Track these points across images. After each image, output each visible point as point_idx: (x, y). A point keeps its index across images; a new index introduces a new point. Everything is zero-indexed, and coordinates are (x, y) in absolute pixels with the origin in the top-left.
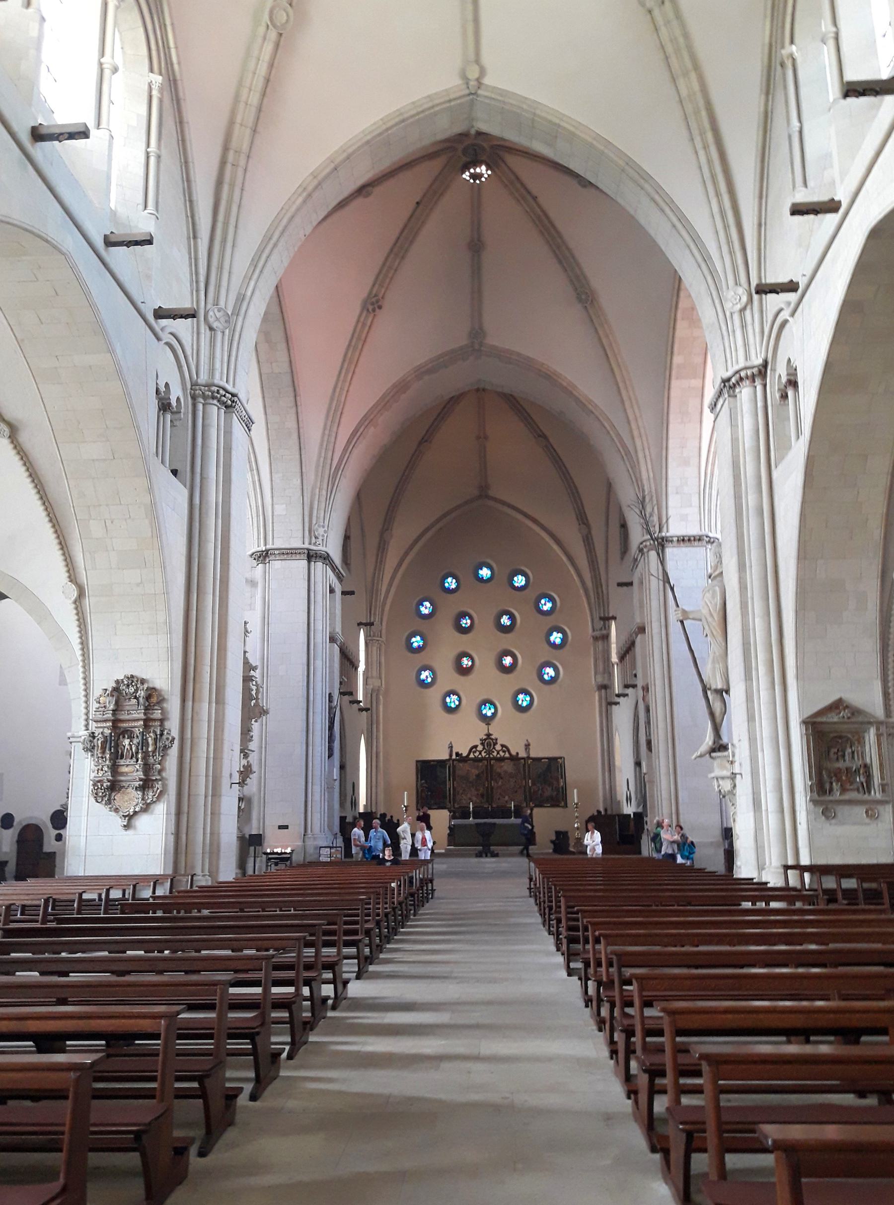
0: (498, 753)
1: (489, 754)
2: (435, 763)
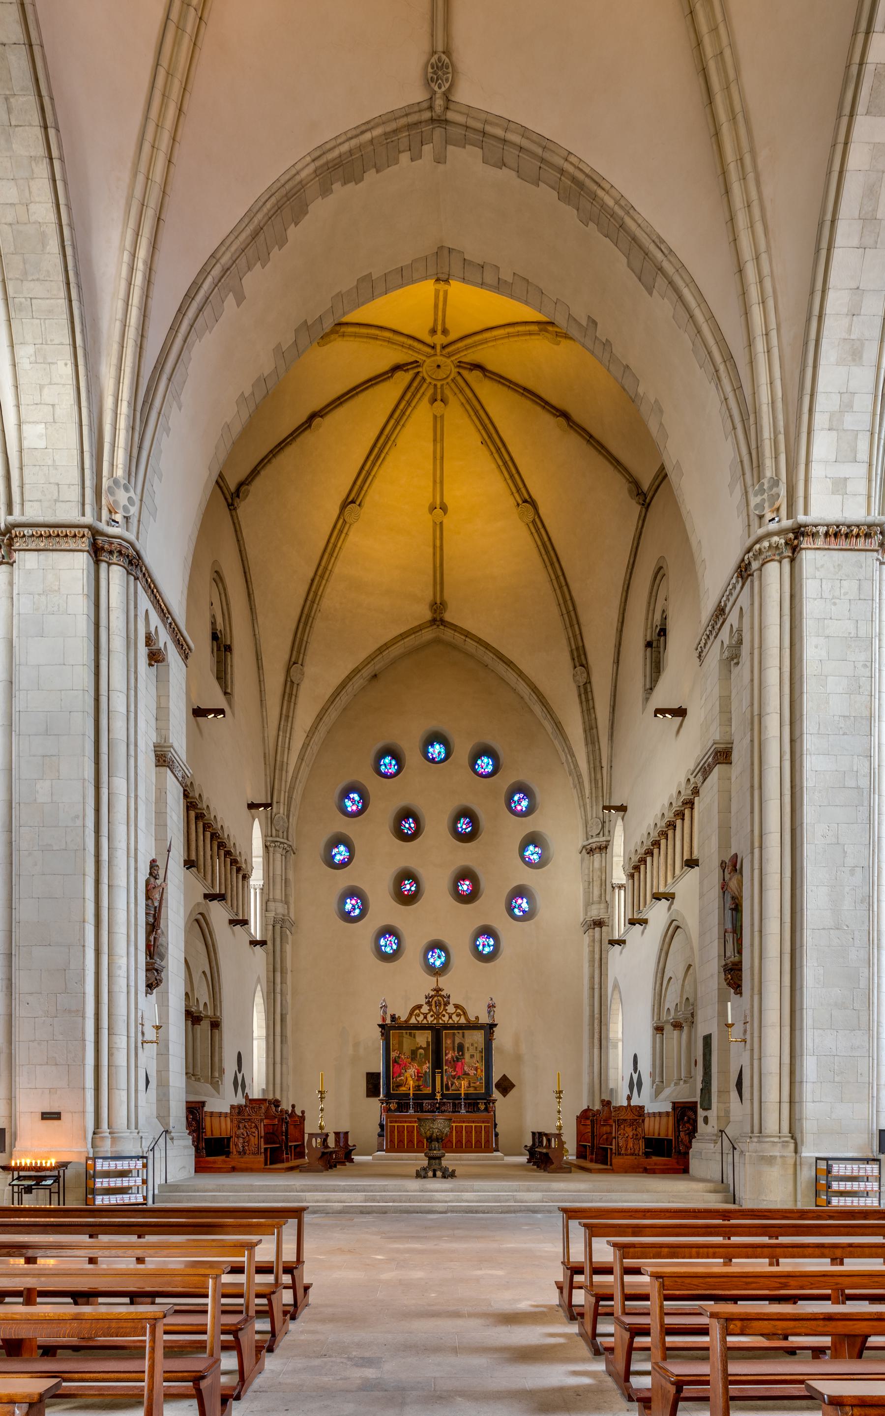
0: (450, 1017)
1: (438, 1018)
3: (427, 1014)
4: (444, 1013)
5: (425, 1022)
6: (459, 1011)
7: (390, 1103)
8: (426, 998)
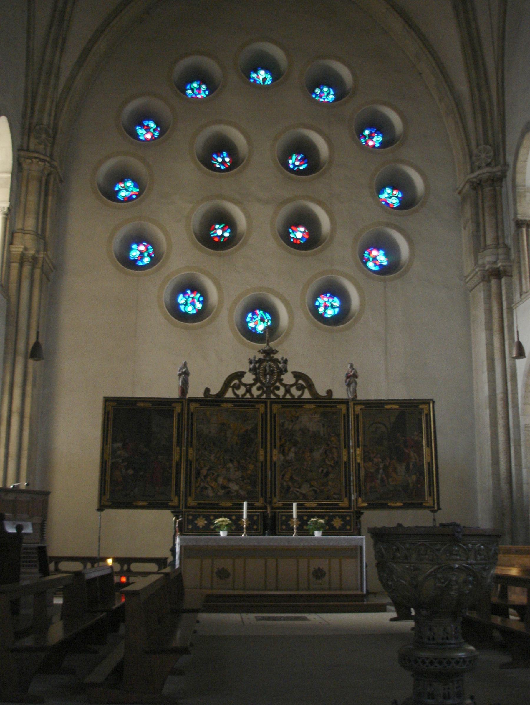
0: (288, 391)
2: (149, 405)
3: (252, 385)
5: (248, 396)
6: (300, 382)
8: (251, 362)
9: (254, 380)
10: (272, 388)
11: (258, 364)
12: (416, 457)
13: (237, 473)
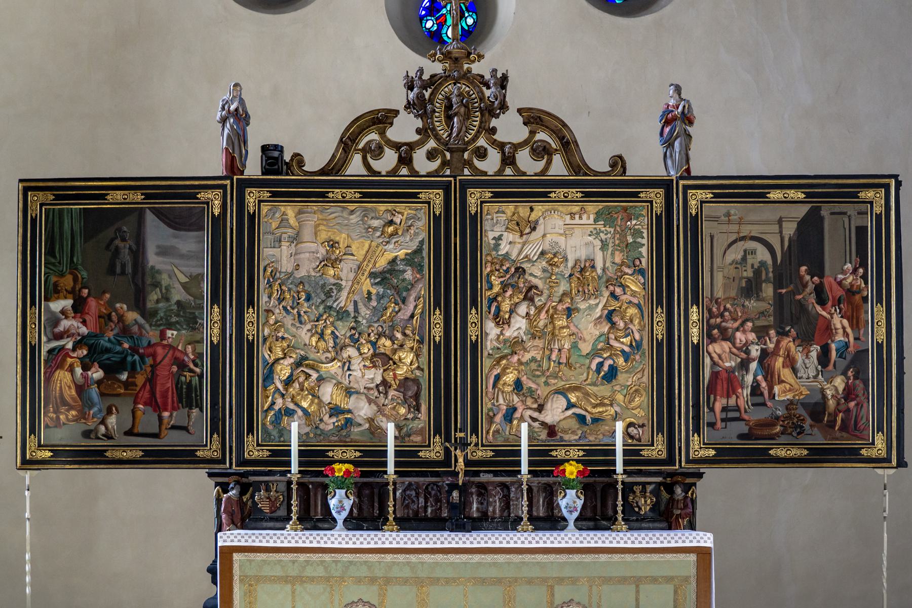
0: (508, 160)
3: (412, 146)
4: (482, 142)
6: (541, 136)
7: (257, 486)
8: (410, 87)
9: (418, 131)
10: (466, 155)
11: (430, 90)
12: (849, 330)
13: (370, 374)
